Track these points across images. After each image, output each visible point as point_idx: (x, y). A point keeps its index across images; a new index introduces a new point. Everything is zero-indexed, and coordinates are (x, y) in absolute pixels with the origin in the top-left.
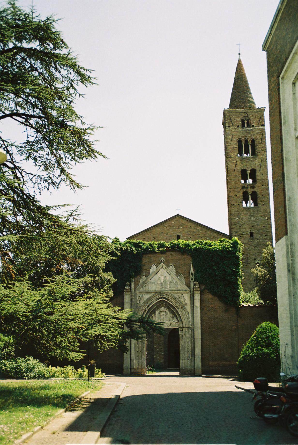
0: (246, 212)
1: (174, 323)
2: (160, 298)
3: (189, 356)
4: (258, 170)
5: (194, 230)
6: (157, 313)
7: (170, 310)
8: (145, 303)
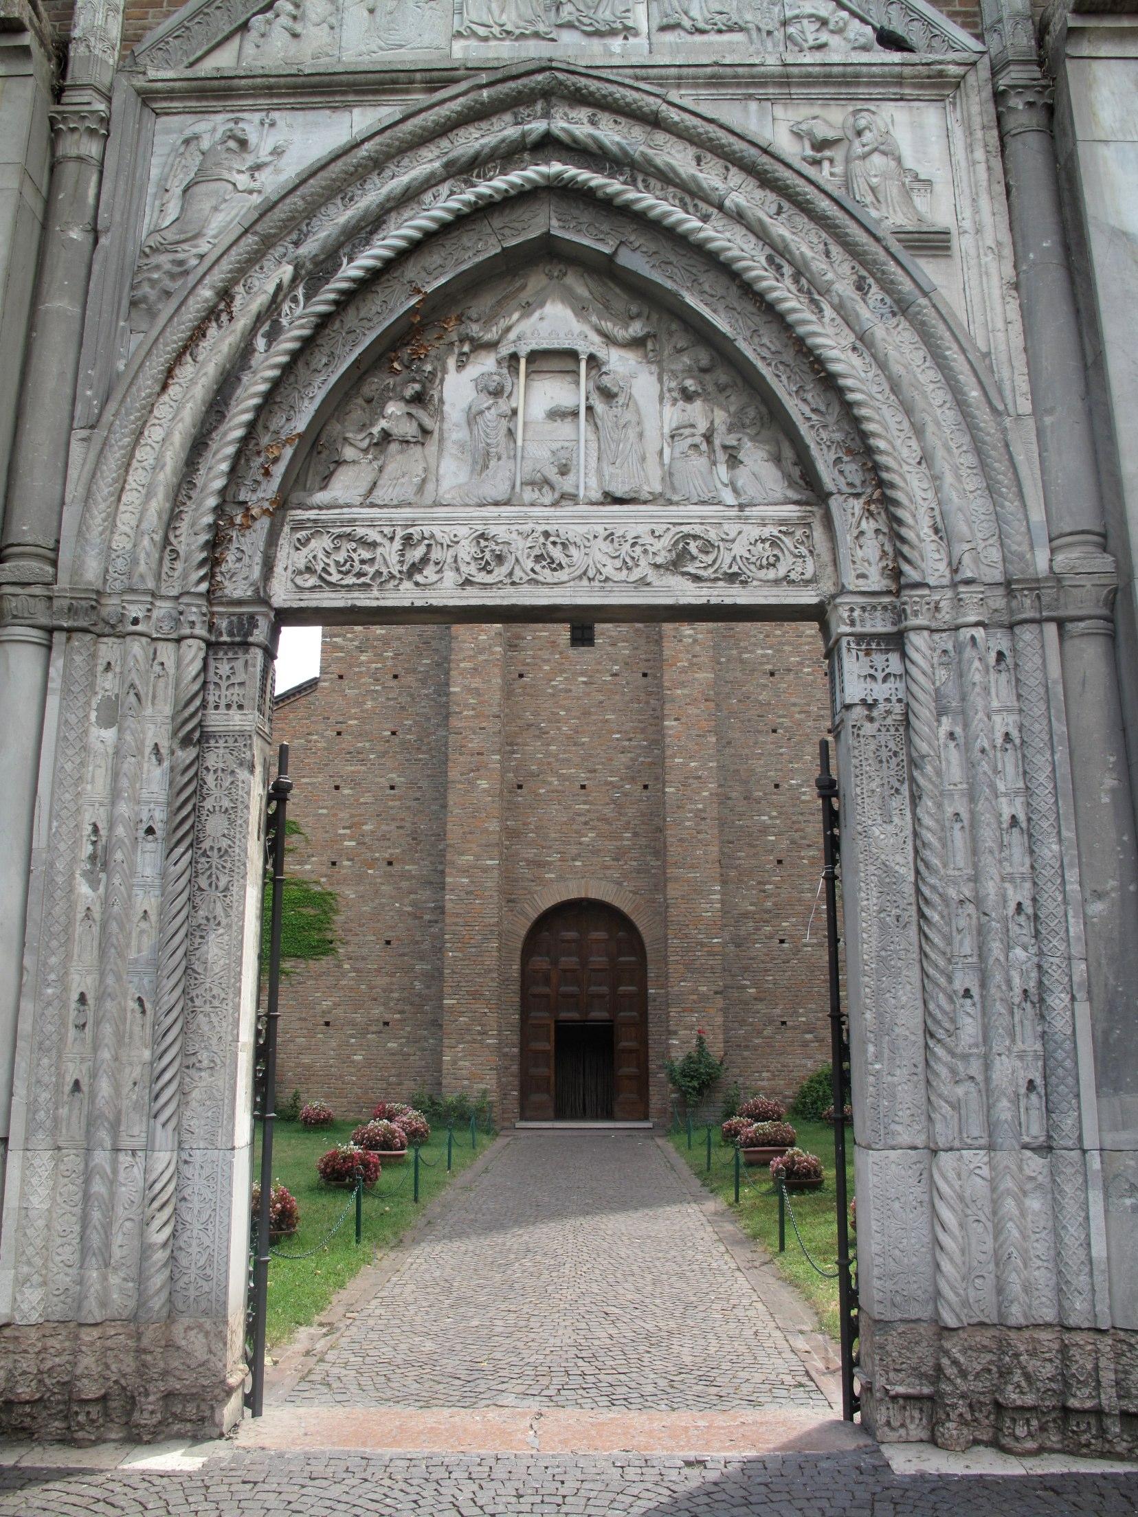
1: (742, 540)
2: (508, 155)
3: (1047, 1088)
6: (459, 387)
7: (661, 320)
8: (273, 226)
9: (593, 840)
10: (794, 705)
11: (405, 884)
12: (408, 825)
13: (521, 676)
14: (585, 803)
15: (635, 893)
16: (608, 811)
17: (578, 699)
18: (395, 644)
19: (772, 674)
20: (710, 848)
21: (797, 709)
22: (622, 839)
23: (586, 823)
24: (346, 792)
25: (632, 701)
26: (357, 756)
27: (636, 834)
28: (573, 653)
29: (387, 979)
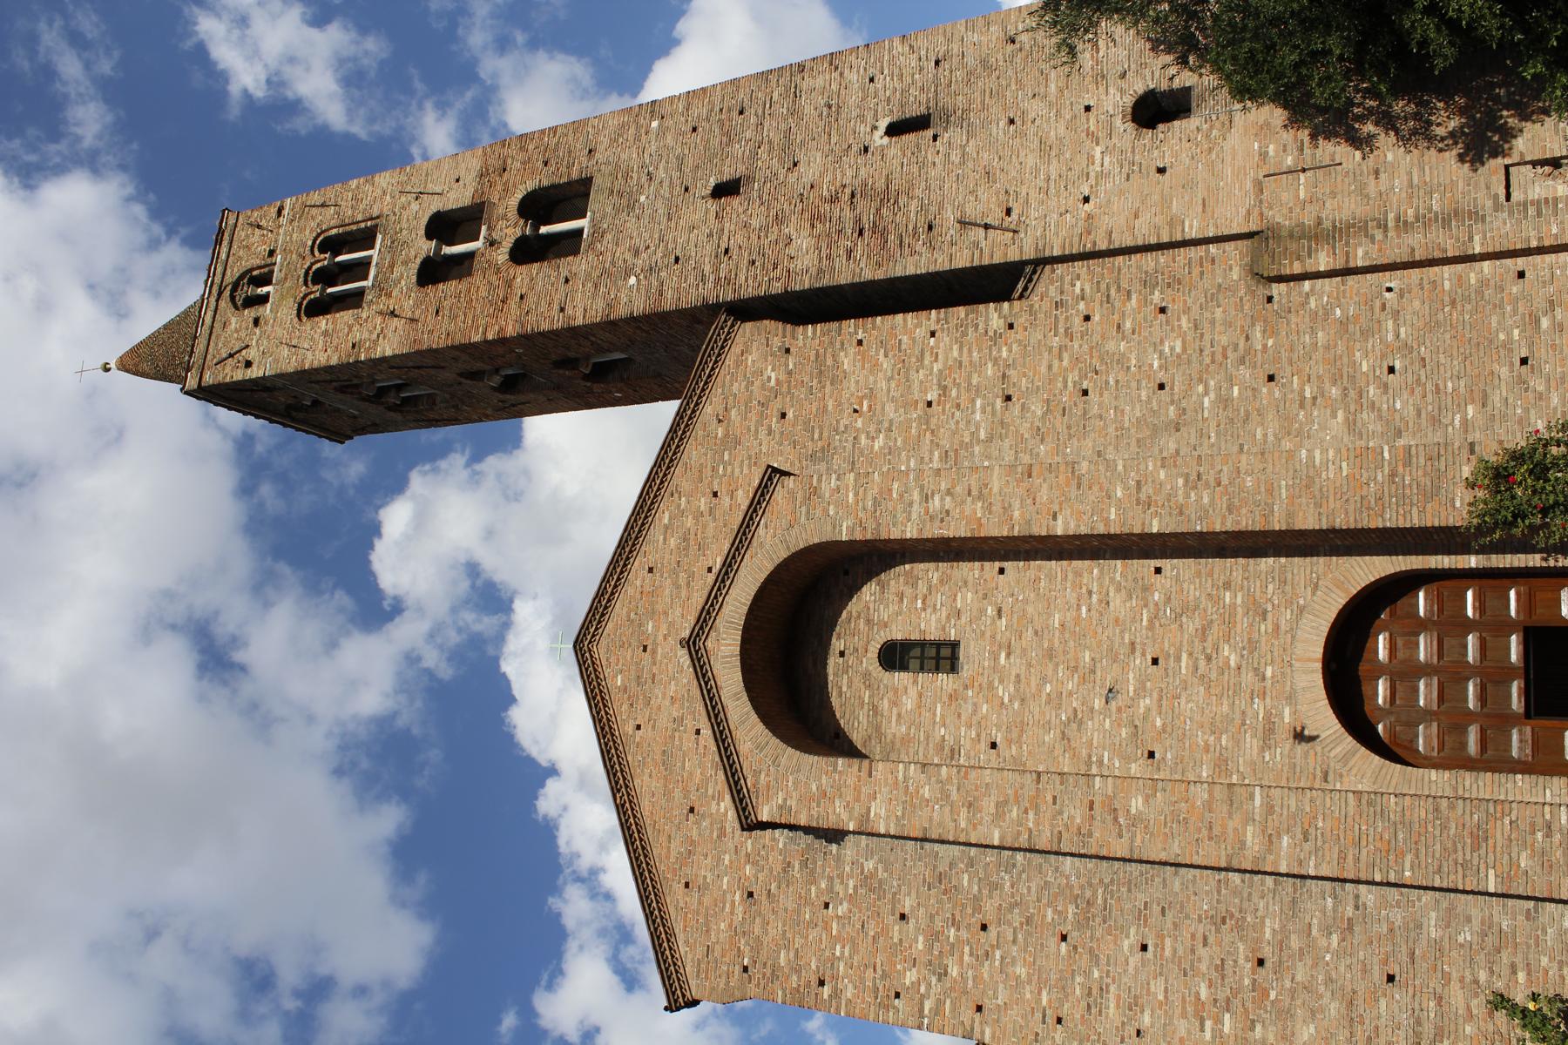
0: (609, 237)
4: (436, 205)
5: (672, 542)
9: (1234, 648)
10: (1050, 367)
11: (1295, 942)
12: (1201, 928)
13: (994, 745)
14: (1178, 659)
15: (1316, 587)
16: (1192, 625)
17: (1030, 665)
18: (938, 923)
19: (1008, 398)
20: (1243, 465)
21: (1056, 363)
22: (1233, 605)
23: (1209, 659)
24: (1147, 1019)
25: (1036, 590)
26: (1094, 999)
27: (1227, 585)
28: (966, 670)
29: (1455, 986)
